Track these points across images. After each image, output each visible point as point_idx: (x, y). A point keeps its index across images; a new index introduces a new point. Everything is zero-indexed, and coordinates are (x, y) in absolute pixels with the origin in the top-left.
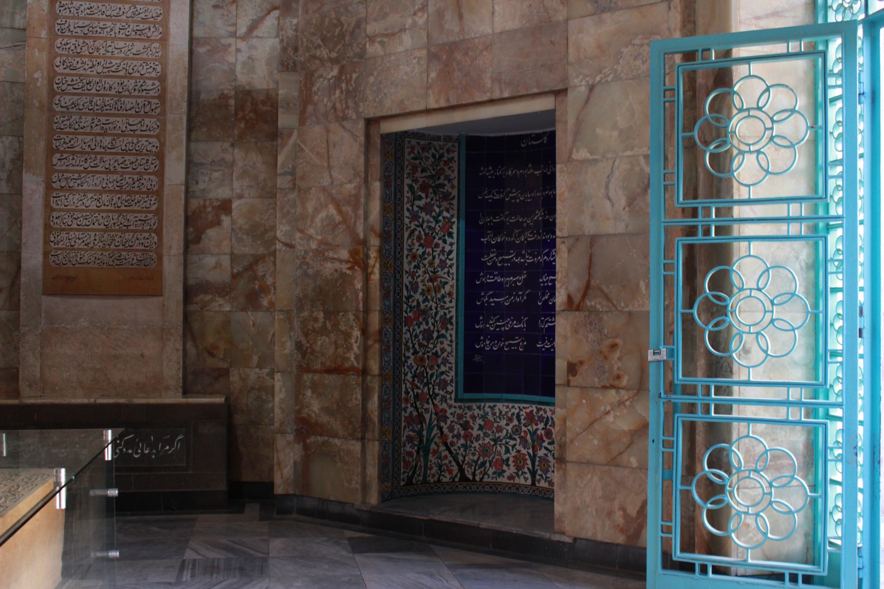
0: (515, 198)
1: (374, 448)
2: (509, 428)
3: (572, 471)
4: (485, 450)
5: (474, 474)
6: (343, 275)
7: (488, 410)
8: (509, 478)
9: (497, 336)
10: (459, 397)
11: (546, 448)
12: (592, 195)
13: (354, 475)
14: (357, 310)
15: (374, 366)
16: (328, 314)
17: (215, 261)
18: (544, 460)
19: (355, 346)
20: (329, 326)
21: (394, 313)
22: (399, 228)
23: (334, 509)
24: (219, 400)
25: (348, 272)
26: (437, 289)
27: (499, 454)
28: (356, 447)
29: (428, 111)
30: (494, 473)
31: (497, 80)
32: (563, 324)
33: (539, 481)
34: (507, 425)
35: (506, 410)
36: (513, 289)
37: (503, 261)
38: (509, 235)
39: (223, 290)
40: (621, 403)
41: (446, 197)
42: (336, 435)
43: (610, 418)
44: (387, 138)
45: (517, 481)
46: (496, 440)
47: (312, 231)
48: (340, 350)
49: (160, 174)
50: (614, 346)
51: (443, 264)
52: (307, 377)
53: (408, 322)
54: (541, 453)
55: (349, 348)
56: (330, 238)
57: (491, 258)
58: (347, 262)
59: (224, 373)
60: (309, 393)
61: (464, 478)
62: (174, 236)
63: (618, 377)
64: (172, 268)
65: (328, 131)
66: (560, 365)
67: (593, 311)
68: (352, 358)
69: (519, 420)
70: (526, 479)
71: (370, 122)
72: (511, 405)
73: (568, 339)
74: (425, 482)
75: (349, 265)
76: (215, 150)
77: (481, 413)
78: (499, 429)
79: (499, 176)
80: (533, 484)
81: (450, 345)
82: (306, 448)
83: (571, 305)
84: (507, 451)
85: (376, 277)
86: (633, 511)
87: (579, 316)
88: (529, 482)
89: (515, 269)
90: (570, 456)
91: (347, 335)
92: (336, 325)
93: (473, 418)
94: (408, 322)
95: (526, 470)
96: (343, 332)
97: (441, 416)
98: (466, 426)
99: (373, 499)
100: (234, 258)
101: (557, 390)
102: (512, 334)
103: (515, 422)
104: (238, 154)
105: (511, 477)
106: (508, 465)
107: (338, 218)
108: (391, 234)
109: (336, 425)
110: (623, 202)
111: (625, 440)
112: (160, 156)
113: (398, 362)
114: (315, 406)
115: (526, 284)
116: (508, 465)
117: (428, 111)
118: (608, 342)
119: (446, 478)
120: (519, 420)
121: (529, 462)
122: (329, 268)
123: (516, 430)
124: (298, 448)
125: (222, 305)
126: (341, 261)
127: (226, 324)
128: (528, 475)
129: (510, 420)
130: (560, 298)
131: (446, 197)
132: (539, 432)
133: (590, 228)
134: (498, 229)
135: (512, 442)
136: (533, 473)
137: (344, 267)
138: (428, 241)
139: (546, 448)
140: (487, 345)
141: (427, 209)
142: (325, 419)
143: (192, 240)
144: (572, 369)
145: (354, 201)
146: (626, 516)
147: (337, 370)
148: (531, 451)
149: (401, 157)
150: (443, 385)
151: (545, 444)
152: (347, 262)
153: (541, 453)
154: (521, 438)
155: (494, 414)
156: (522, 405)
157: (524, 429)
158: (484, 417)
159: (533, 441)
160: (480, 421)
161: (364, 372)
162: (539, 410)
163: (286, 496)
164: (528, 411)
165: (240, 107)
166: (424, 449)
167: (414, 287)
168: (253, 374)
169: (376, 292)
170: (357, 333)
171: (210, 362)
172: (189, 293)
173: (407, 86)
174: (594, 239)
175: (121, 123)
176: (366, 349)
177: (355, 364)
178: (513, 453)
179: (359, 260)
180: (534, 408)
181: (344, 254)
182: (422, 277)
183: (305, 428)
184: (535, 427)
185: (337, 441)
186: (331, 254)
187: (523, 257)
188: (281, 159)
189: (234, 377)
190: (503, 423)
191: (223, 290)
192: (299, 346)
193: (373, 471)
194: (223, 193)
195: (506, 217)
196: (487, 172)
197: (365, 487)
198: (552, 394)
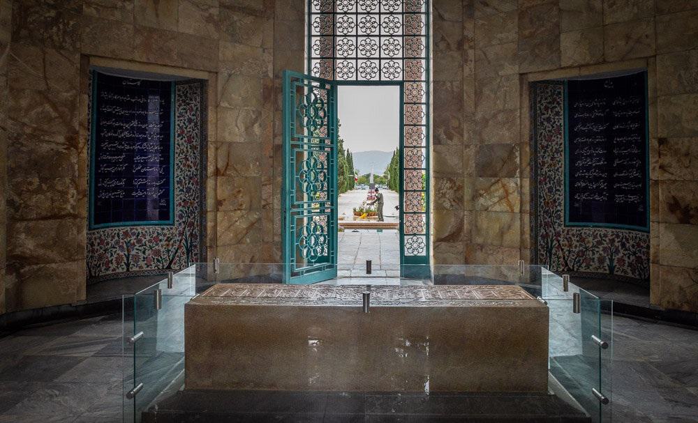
0: (118, 112)
2: (113, 242)
5: (95, 273)
6: (58, 153)
7: (102, 233)
8: (113, 271)
9: (108, 190)
10: (92, 228)
11: (137, 249)
14: (74, 176)
16: (43, 180)
19: (72, 201)
20: (44, 187)
25: (66, 151)
27: (107, 258)
30: (105, 269)
33: (132, 268)
34: (112, 240)
36: (116, 164)
37: (111, 147)
38: (115, 132)
40: (243, 216)
42: (54, 261)
43: (238, 223)
45: (117, 271)
46: (105, 251)
48: (57, 204)
50: (239, 191)
54: (133, 252)
55: (66, 201)
56: (46, 127)
57: (105, 145)
58: (64, 144)
63: (241, 205)
65: (44, 53)
67: (229, 176)
69: (119, 236)
70: (123, 269)
72: (114, 229)
75: (65, 146)
77: (99, 235)
80: (128, 270)
84: (112, 255)
88: (125, 270)
89: (119, 152)
91: (63, 194)
92: (52, 188)
93: (95, 239)
95: (123, 264)
96: (59, 191)
99: (83, 297)
102: (116, 188)
103: (116, 238)
105: (114, 270)
106: (112, 263)
107: (54, 114)
109: (51, 254)
110: (243, 129)
111: (244, 232)
115: (125, 161)
116: (112, 263)
118: (237, 190)
120: (119, 236)
121: (125, 259)
123: (117, 243)
126: (57, 144)
128: (125, 266)
129: (113, 237)
132: (132, 242)
134: (110, 128)
135: (114, 250)
137: (61, 148)
139: (137, 249)
142: (41, 252)
144: (219, 203)
147: (54, 217)
148: (126, 253)
151: (137, 247)
152: (64, 144)
153: (133, 252)
154: (120, 246)
155: (105, 235)
156: (120, 228)
157: (121, 241)
158: (100, 238)
159: (128, 247)
160: (98, 241)
162: (131, 229)
164: (124, 231)
177: (72, 211)
178: (115, 256)
179: (72, 142)
180: (128, 228)
181: (61, 139)
184: (129, 239)
185: (53, 265)
186: (47, 138)
187: (123, 145)
190: (109, 240)
195: (113, 122)
197: (79, 290)
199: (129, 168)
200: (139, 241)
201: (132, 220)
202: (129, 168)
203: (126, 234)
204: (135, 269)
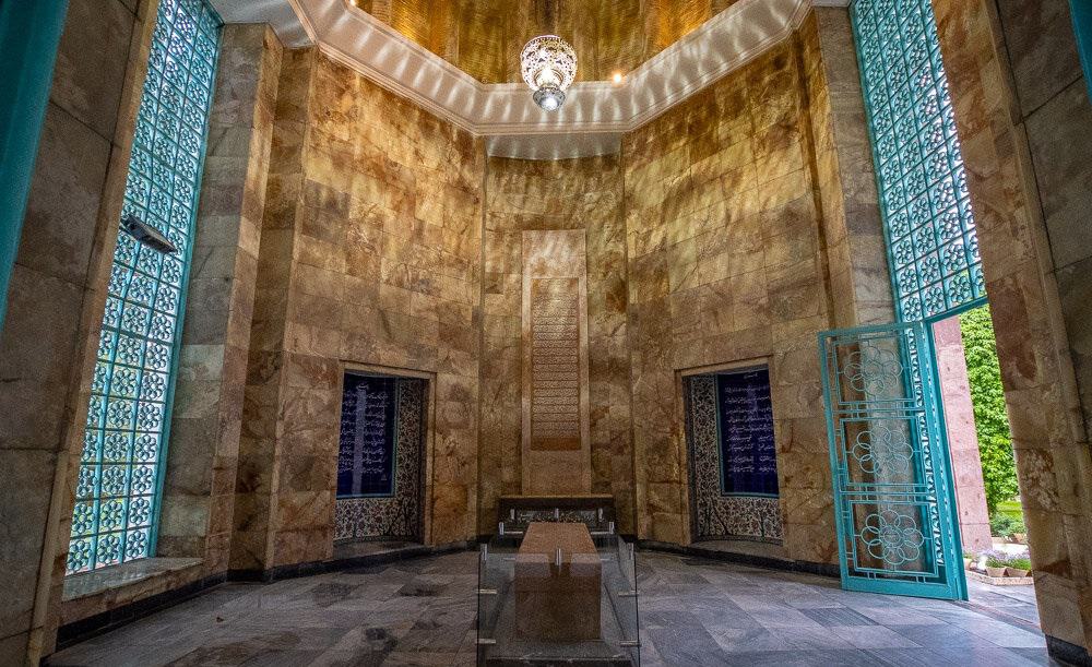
1: (687, 518)
3: (792, 528)
4: (736, 520)
12: (788, 403)
13: (678, 529)
15: (685, 480)
17: (603, 436)
18: (768, 525)
21: (692, 456)
22: (691, 418)
23: (668, 546)
24: (611, 496)
26: (709, 444)
28: (679, 517)
29: (705, 366)
31: (738, 350)
32: (780, 460)
35: (748, 501)
39: (607, 447)
41: (710, 402)
44: (687, 380)
47: (651, 420)
49: (578, 396)
50: (808, 469)
51: (711, 433)
52: (652, 485)
53: (698, 459)
54: (766, 520)
55: (672, 472)
59: (608, 484)
60: (653, 492)
61: (727, 533)
62: (585, 424)
63: (812, 483)
64: (585, 437)
66: (781, 478)
67: (795, 453)
68: (674, 476)
71: (676, 371)
73: (784, 467)
74: (709, 535)
76: (600, 385)
78: (743, 509)
79: (739, 393)
81: (716, 470)
82: (653, 518)
83: (784, 450)
85: (683, 439)
86: (826, 545)
87: (789, 455)
90: (790, 519)
94: (698, 459)
97: (715, 502)
98: (727, 508)
100: (612, 432)
101: (780, 491)
104: (611, 386)
108: (689, 421)
109: (668, 507)
111: (819, 513)
112: (578, 389)
113: (694, 477)
114: (656, 499)
115: (752, 441)
117: (705, 366)
119: (719, 533)
122: (660, 435)
123: (752, 510)
124: (649, 518)
125: (607, 453)
127: (609, 462)
130: (778, 446)
131: (710, 402)
133: (791, 415)
136: (763, 531)
138: (703, 422)
140: (736, 470)
141: (703, 408)
142: (662, 504)
143: (593, 425)
145: (671, 406)
146: (823, 549)
149: (690, 385)
150: (715, 488)
161: (680, 483)
163: (644, 540)
165: (611, 366)
166: (708, 518)
167: (699, 444)
168: (623, 484)
169: (684, 446)
170: (676, 465)
171: (602, 479)
172: (593, 448)
173: (695, 357)
174: (793, 421)
175: (561, 375)
176: (680, 472)
179: (674, 431)
181: (668, 429)
182: (702, 438)
183: (652, 508)
188: (634, 388)
189: (613, 485)
191: (607, 447)
192: (647, 471)
193: (687, 528)
194: (605, 403)
196: (728, 390)
198: (778, 493)
199: (755, 447)
200: (769, 511)
201: (761, 492)
202: (755, 447)
203: (759, 504)
204: (768, 536)
